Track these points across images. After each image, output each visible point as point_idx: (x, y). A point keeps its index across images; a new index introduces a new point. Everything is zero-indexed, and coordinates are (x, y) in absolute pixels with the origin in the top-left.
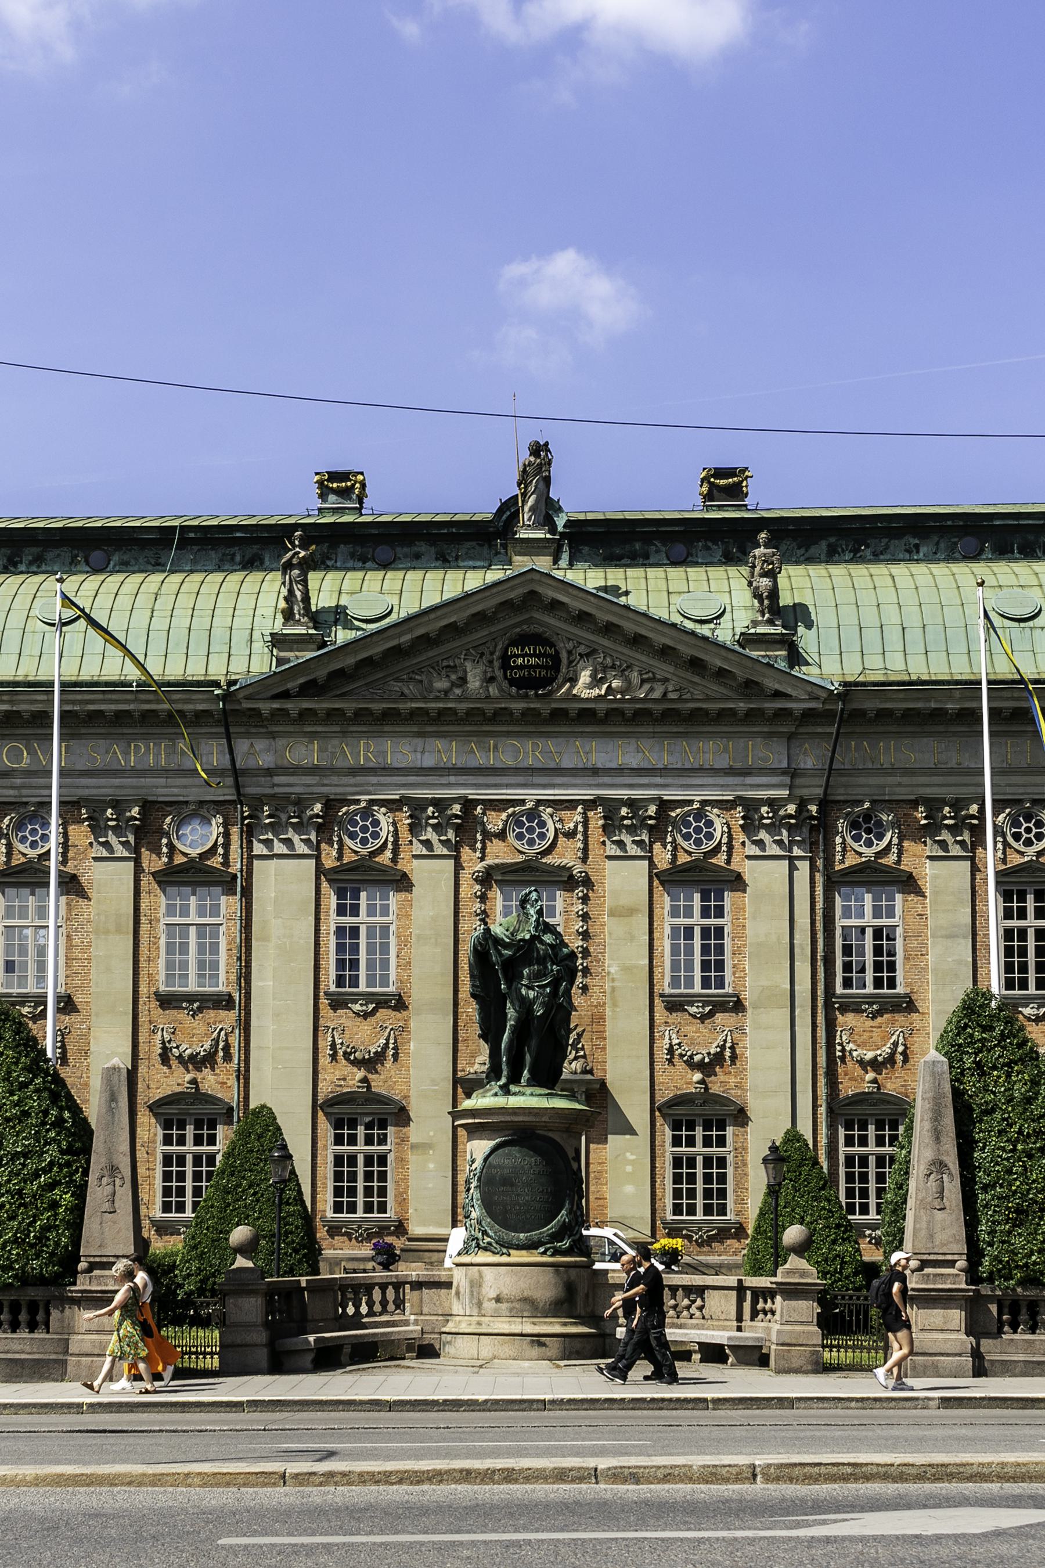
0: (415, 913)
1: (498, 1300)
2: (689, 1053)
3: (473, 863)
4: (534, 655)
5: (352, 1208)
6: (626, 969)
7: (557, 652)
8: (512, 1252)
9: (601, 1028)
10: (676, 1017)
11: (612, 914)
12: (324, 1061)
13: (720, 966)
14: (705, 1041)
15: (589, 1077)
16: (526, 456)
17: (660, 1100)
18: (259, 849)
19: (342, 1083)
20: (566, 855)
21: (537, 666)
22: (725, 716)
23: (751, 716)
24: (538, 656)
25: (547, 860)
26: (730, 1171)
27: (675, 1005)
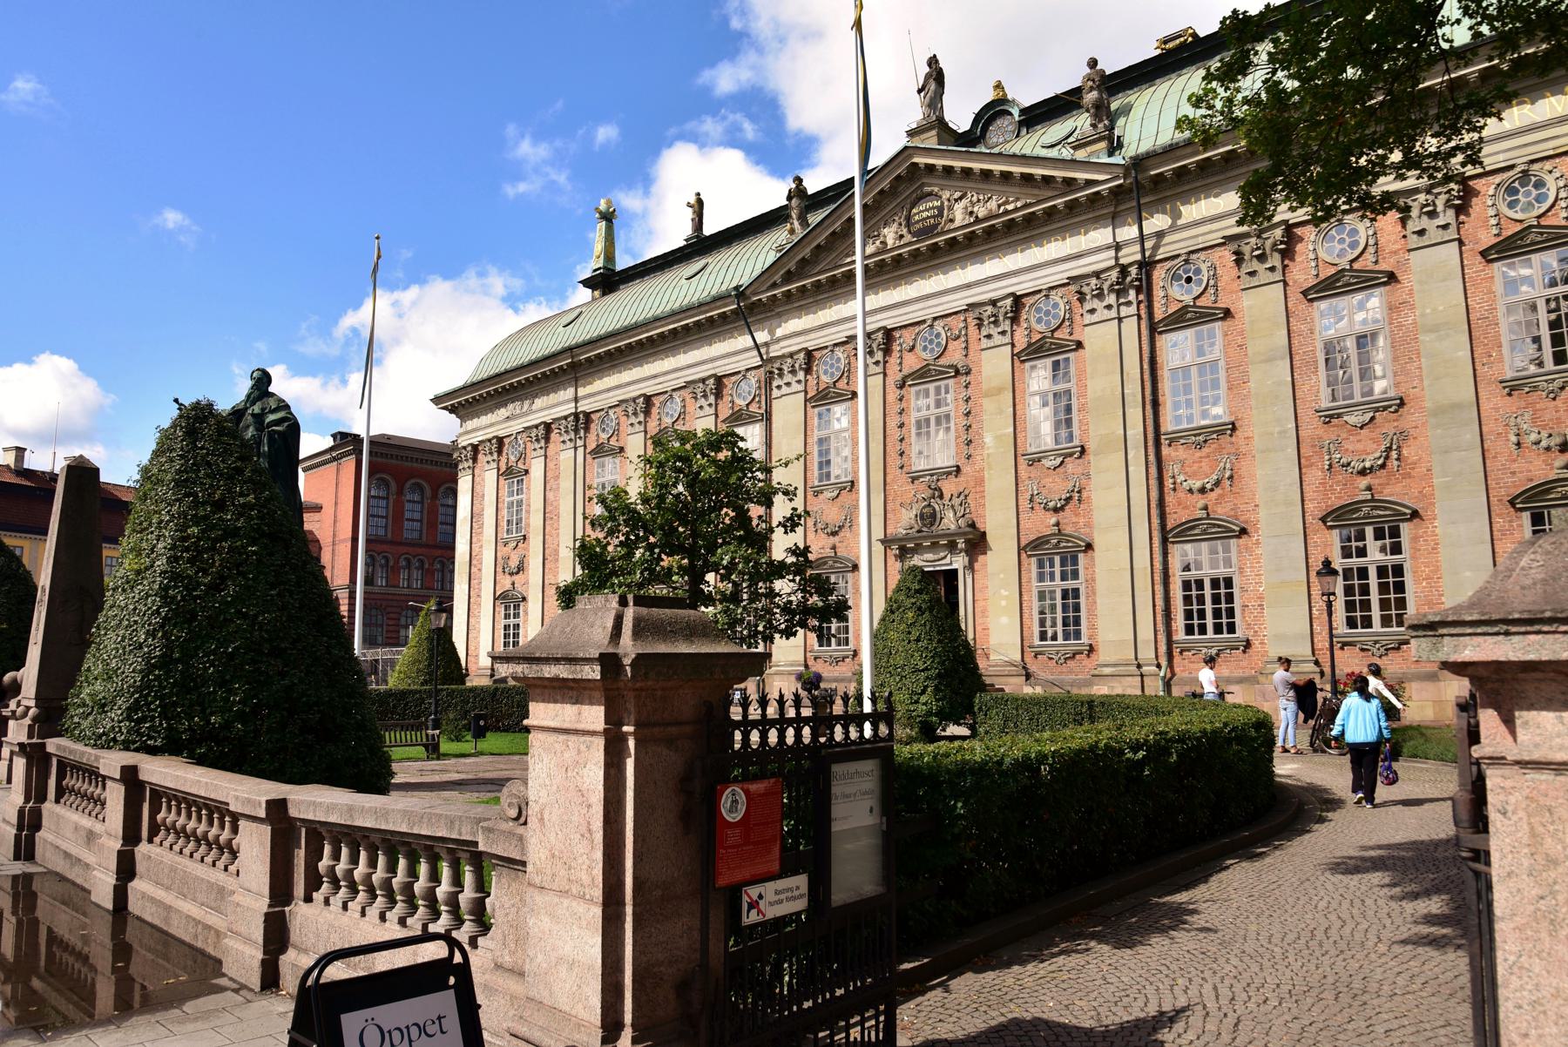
3: (894, 375)
6: (998, 438)
10: (1034, 471)
14: (1057, 488)
17: (1023, 544)
20: (955, 356)
22: (1051, 213)
23: (1072, 206)
26: (1082, 600)
27: (1034, 461)
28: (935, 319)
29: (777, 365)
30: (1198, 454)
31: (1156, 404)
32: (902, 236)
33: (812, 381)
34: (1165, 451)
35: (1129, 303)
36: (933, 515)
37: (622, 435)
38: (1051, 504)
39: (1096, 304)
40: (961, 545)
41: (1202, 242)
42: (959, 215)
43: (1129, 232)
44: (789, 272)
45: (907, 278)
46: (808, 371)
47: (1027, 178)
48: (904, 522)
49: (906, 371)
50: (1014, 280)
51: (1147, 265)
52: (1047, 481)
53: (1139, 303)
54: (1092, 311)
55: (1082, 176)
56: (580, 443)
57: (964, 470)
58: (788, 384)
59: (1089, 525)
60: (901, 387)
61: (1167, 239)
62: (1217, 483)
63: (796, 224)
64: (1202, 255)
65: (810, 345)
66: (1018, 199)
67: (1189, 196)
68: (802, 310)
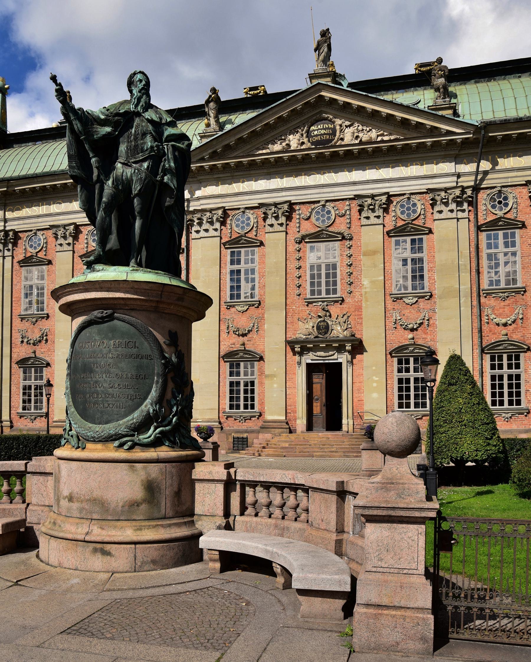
0: (268, 261)
1: (71, 499)
2: (406, 324)
3: (294, 234)
4: (323, 129)
5: (238, 407)
6: (372, 282)
7: (335, 127)
8: (89, 445)
9: (360, 313)
11: (364, 255)
12: (224, 335)
13: (422, 277)
15: (353, 338)
16: (319, 37)
17: (390, 348)
18: (194, 235)
19: (233, 346)
20: (341, 226)
21: (325, 134)
24: (325, 129)
25: (330, 229)
27: (397, 299)
28: (327, 201)
29: (198, 215)
30: (503, 304)
31: (478, 272)
32: (303, 143)
33: (226, 231)
34: (483, 300)
35: (463, 211)
36: (327, 327)
37: (50, 252)
38: (410, 326)
39: (443, 207)
40: (348, 347)
41: (510, 182)
42: (348, 136)
43: (471, 167)
44: (215, 152)
45: (308, 172)
46: (223, 223)
47: (405, 122)
48: (304, 329)
49: (303, 232)
50: (387, 185)
51: (476, 189)
52: (406, 312)
53: (470, 211)
54: (440, 212)
55: (445, 127)
56: (7, 253)
57: (347, 300)
58: (206, 231)
59: (433, 340)
60: (300, 243)
61: (489, 176)
62: (514, 322)
63: (212, 121)
64: (509, 189)
65: (227, 205)
66: (391, 134)
67: (506, 154)
68: (217, 182)
